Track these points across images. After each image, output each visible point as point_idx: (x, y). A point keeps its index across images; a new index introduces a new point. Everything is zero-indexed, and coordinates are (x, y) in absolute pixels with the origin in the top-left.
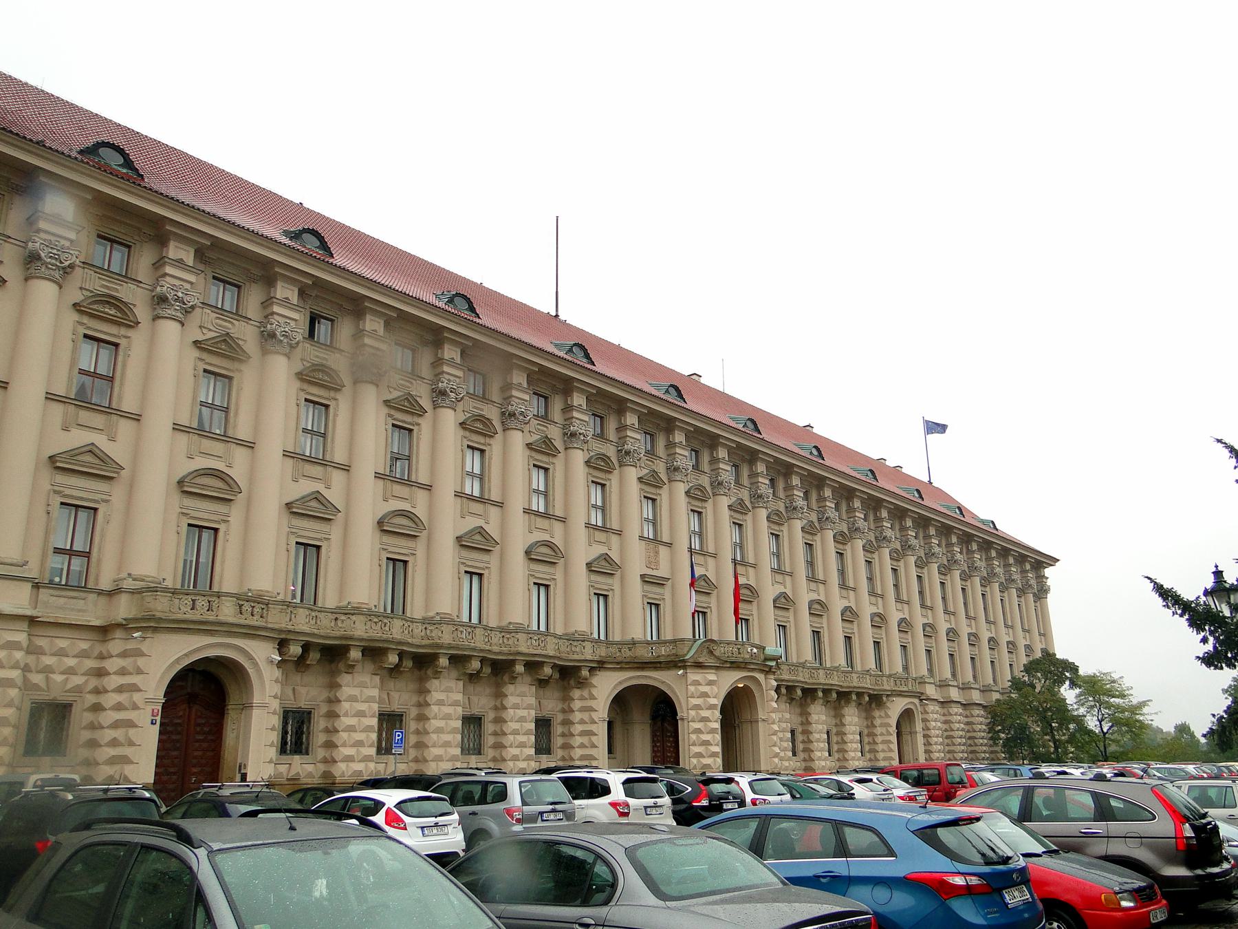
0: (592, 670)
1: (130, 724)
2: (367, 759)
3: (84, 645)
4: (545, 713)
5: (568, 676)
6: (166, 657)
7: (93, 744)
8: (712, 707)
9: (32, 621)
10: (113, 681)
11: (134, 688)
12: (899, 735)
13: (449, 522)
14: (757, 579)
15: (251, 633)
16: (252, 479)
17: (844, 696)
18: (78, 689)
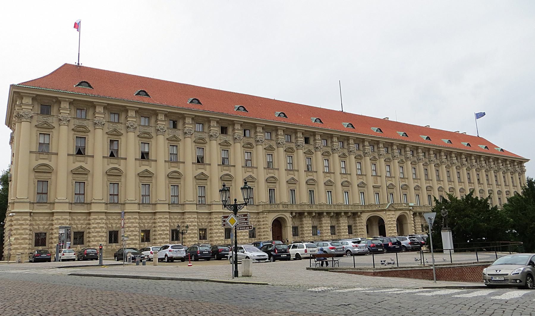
0: (361, 213)
1: (267, 231)
2: (311, 237)
4: (350, 224)
5: (355, 215)
6: (272, 217)
8: (394, 221)
13: (322, 179)
15: (286, 211)
16: (279, 177)
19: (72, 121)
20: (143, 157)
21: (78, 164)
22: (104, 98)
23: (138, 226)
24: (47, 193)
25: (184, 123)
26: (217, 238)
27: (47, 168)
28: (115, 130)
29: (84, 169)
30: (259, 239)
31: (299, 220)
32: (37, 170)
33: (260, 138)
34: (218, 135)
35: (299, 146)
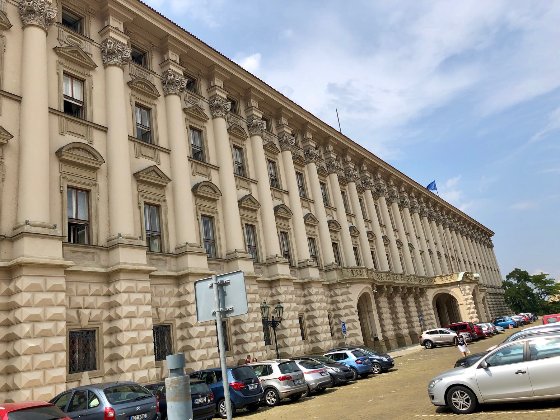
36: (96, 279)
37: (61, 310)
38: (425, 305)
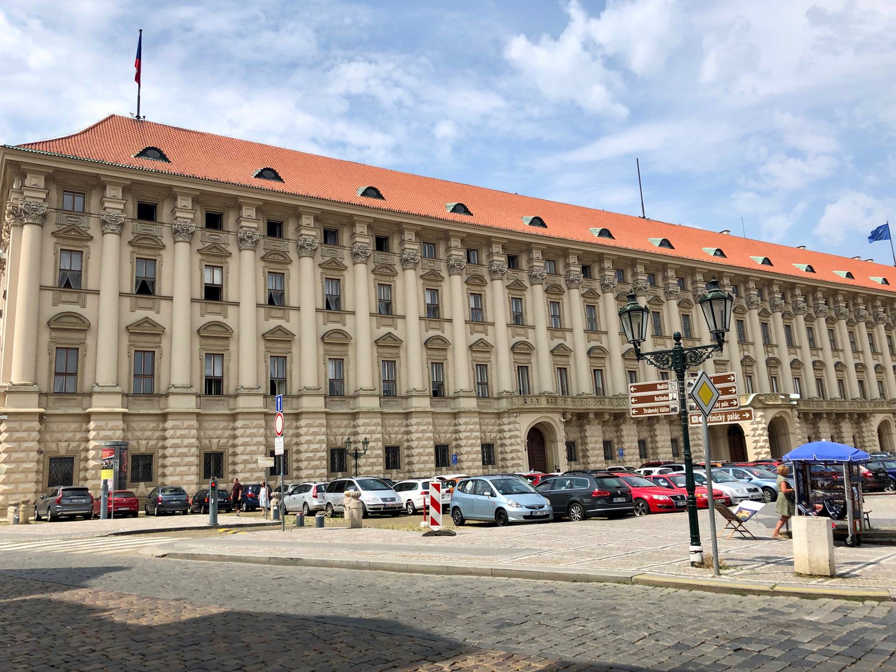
3: (493, 421)
6: (525, 423)
7: (504, 459)
9: (480, 413)
10: (507, 435)
11: (517, 437)
12: (880, 436)
14: (779, 353)
15: (553, 411)
17: (840, 416)
18: (495, 439)
19: (130, 226)
20: (271, 301)
21: (140, 314)
22: (193, 179)
23: (264, 442)
24: (75, 374)
25: (353, 235)
26: (422, 466)
27: (75, 320)
28: (215, 246)
29: (154, 325)
30: (503, 467)
31: (577, 429)
32: (56, 324)
33: (498, 266)
34: (418, 258)
35: (572, 281)
36: (448, 416)
37: (431, 435)
38: (867, 431)
